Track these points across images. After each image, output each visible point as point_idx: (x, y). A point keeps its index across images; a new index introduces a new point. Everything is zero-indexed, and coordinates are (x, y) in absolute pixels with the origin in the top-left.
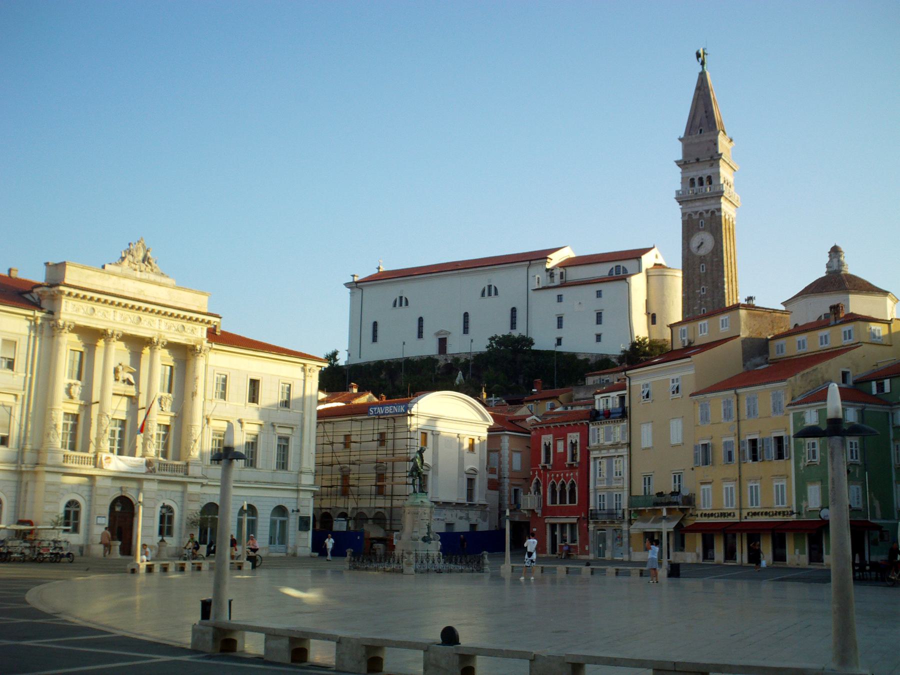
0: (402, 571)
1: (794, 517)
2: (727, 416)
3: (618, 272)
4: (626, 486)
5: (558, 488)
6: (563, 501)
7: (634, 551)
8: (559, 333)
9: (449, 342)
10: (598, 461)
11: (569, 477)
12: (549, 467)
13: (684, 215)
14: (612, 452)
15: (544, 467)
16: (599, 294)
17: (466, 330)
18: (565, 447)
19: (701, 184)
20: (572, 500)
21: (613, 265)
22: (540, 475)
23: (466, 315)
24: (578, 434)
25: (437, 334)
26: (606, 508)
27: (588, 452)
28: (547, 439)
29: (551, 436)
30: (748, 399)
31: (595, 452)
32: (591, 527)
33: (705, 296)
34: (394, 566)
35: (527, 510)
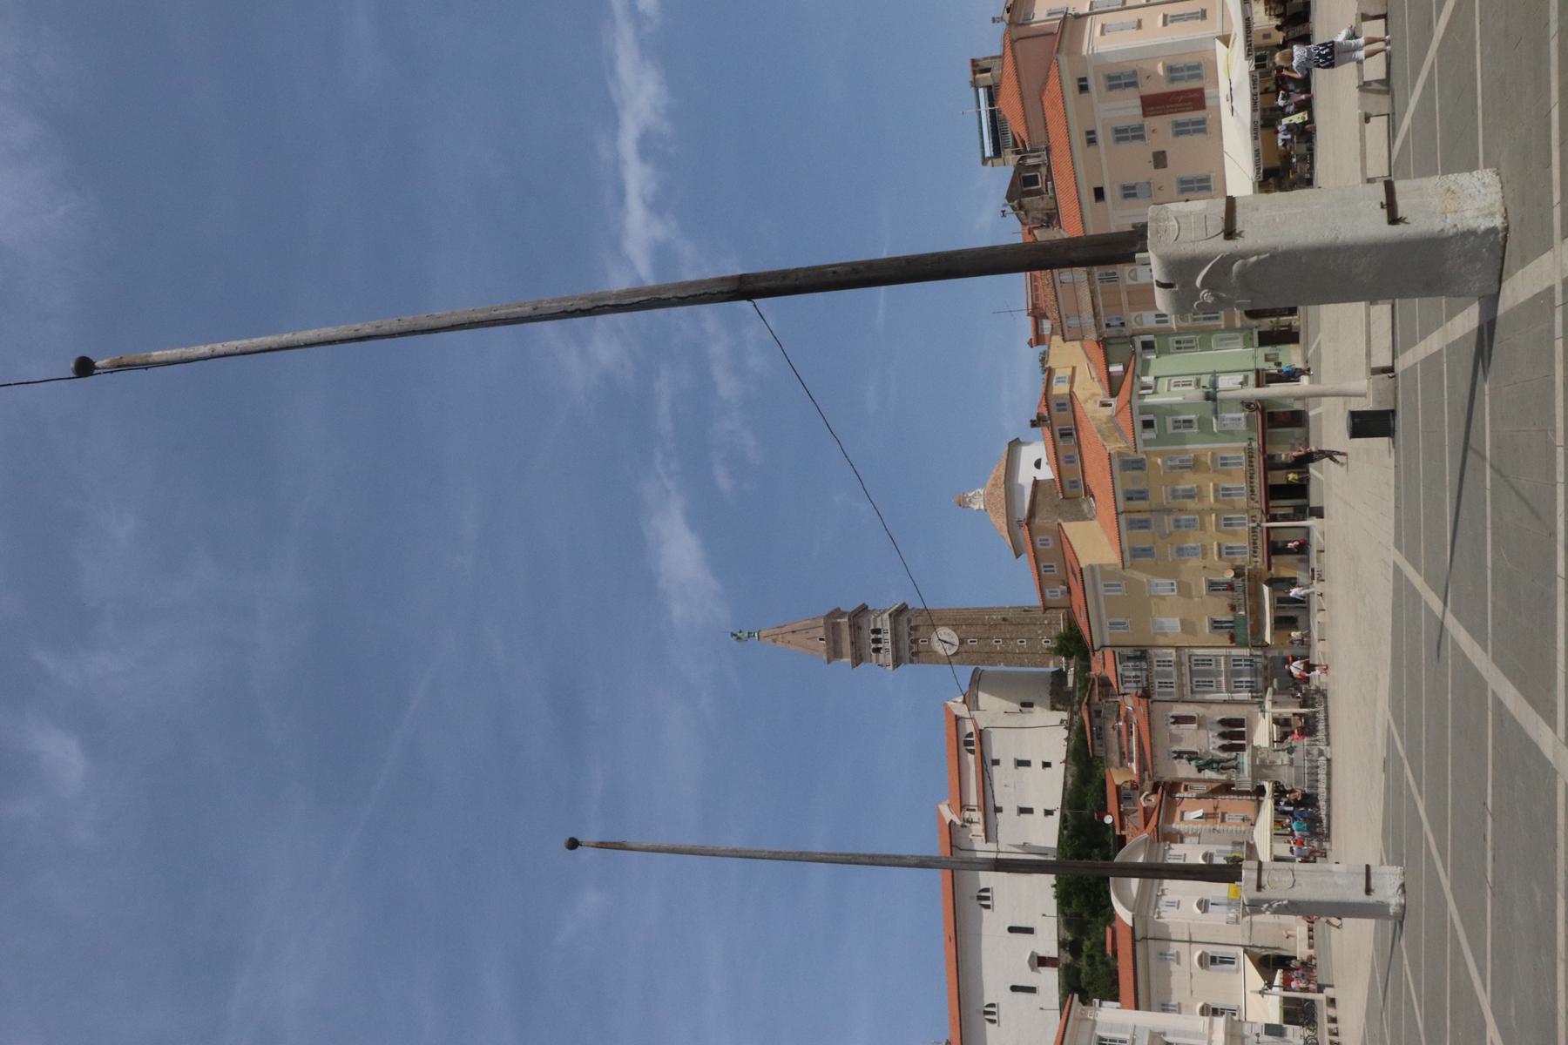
0: (1329, 760)
1: (1255, 444)
2: (1144, 524)
3: (971, 743)
4: (1223, 651)
8: (1039, 812)
9: (1042, 954)
13: (912, 662)
14: (1185, 670)
16: (996, 762)
17: (1029, 931)
19: (877, 641)
21: (963, 749)
23: (1012, 930)
25: (1033, 969)
30: (1130, 499)
33: (1005, 639)
34: (1322, 776)
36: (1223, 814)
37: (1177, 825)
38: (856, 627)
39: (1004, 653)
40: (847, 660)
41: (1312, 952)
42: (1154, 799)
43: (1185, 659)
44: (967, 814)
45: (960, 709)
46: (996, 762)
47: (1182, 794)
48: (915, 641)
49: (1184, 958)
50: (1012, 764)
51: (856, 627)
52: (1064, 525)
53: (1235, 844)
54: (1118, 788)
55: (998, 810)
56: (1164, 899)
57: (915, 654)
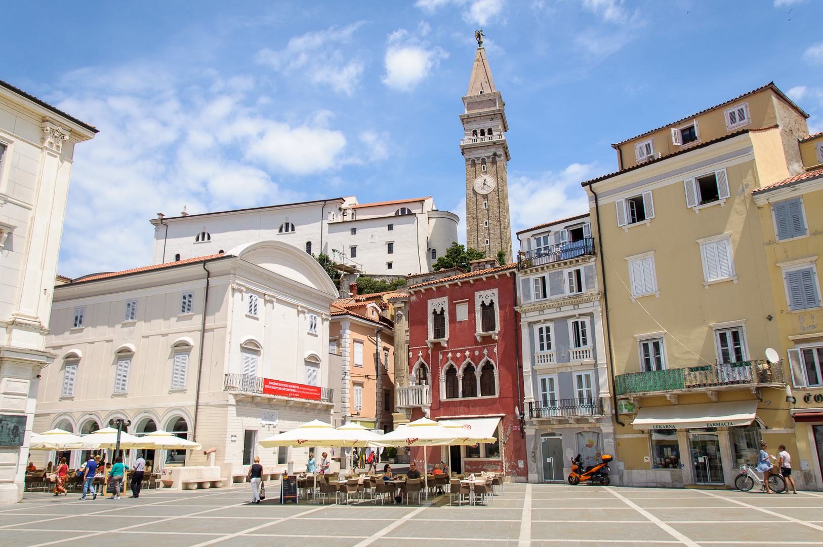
4: (602, 359)
5: (460, 373)
6: (470, 391)
7: (629, 468)
10: (536, 328)
11: (481, 356)
12: (444, 342)
13: (467, 160)
14: (567, 311)
15: (437, 346)
16: (390, 227)
18: (471, 311)
19: (483, 133)
20: (488, 388)
22: (426, 358)
24: (496, 291)
26: (557, 397)
27: (517, 316)
28: (437, 304)
29: (446, 299)
31: (528, 314)
32: (529, 431)
35: (407, 409)
36: (361, 385)
37: (348, 335)
38: (492, 116)
39: (477, 230)
40: (466, 112)
41: (178, 488)
42: (375, 317)
43: (584, 308)
44: (350, 212)
45: (429, 205)
46: (390, 227)
47: (382, 344)
48: (484, 162)
49: (184, 325)
50: (389, 240)
51: (492, 116)
52: (777, 131)
53: (330, 392)
54: (380, 297)
55: (354, 231)
56: (261, 302)
57: (474, 164)
